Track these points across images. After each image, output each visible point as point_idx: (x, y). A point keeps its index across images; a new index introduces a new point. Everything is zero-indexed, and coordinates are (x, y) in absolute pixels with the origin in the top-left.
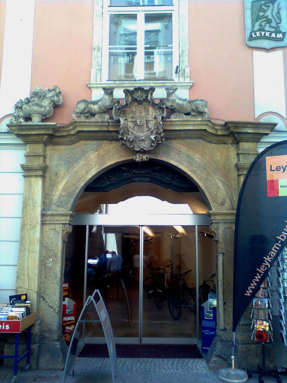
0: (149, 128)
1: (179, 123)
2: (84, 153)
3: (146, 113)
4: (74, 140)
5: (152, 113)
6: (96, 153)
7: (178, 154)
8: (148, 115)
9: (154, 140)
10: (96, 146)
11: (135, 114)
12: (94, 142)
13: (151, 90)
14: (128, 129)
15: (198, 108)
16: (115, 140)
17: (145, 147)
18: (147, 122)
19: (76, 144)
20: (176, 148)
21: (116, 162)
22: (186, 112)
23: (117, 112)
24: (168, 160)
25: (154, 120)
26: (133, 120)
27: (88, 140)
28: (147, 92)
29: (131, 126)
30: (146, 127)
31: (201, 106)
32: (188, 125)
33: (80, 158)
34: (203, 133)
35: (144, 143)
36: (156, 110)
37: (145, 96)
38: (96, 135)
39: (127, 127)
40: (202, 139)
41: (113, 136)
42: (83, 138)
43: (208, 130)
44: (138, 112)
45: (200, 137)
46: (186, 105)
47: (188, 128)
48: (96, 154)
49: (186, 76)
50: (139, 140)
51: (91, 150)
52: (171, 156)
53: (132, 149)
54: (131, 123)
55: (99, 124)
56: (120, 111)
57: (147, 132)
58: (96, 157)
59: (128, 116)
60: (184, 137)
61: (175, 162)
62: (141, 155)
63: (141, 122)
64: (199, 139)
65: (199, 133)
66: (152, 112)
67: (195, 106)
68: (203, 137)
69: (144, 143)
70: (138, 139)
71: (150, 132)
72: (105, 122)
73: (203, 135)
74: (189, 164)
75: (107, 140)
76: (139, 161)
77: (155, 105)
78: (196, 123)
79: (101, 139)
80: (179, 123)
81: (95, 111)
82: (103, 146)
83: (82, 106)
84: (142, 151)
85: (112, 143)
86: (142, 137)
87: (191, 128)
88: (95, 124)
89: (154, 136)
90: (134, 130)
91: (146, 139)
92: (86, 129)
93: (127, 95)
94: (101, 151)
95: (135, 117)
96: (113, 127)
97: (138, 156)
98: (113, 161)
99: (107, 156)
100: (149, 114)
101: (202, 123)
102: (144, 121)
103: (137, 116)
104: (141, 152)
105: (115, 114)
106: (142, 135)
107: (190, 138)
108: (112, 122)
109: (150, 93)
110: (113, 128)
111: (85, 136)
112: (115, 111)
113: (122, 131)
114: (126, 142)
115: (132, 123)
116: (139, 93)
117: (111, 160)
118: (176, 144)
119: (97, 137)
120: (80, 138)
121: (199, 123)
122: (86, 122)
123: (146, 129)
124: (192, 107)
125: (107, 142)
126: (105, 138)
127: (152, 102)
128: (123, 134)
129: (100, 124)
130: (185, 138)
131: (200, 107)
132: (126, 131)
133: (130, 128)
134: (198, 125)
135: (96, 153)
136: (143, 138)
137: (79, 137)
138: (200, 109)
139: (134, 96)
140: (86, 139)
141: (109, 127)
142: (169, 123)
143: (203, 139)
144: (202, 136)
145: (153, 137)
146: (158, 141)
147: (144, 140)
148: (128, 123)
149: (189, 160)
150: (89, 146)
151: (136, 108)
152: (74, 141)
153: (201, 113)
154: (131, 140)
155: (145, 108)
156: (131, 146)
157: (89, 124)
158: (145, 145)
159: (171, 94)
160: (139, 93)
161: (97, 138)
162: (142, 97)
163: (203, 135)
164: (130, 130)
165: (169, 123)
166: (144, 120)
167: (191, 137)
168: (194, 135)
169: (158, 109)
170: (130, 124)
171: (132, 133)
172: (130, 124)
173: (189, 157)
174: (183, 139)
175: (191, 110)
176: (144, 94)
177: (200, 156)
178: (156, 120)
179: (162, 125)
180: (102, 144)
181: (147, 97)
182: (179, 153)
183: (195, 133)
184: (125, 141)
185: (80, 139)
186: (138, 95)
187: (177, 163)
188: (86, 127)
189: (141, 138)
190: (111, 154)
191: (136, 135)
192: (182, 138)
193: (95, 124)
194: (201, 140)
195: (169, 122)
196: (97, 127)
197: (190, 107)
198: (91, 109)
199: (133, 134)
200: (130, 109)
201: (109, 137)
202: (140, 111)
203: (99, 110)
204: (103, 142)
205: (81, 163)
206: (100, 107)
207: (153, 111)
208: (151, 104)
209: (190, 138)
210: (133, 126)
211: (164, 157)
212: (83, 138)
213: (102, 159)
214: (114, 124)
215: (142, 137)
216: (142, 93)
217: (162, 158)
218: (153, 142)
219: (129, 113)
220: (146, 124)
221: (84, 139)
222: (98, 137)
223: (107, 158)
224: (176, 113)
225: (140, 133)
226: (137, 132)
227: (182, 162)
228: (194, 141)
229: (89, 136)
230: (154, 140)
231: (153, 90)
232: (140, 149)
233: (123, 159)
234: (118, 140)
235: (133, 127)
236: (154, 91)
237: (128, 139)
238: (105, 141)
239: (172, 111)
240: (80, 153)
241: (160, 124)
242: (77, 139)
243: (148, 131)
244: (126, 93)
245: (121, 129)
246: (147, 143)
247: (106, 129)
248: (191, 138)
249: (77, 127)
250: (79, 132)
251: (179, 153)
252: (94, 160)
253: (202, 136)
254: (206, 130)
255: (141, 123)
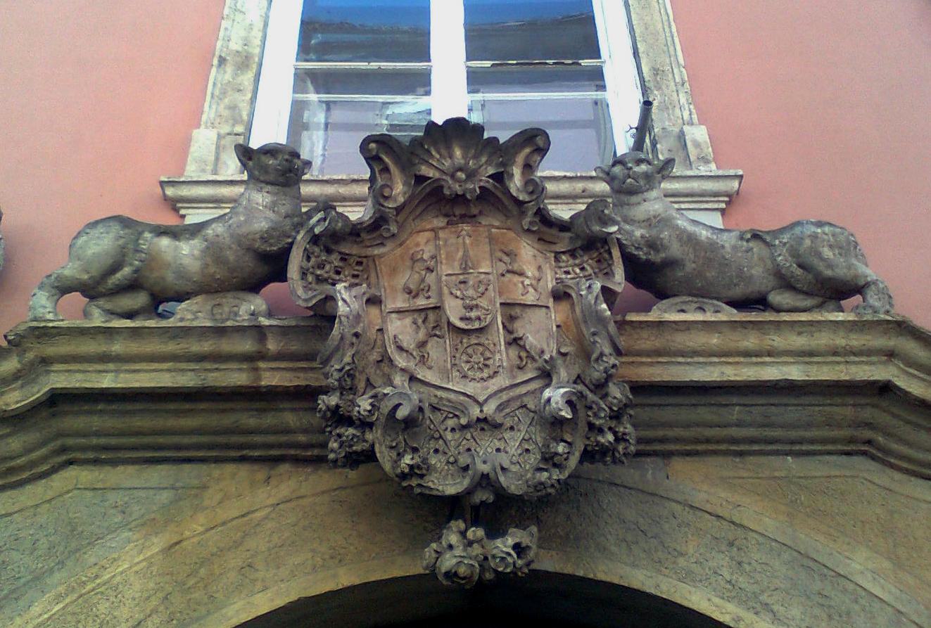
0: (523, 348)
1: (714, 340)
2: (75, 541)
3: (502, 267)
4: (19, 461)
5: (539, 268)
6: (157, 544)
7: (731, 544)
8: (516, 279)
9: (566, 414)
10: (165, 496)
11: (430, 270)
12: (157, 475)
13: (522, 147)
14: (385, 359)
15: (815, 262)
16: (297, 461)
17: (503, 469)
18: (512, 311)
19: (29, 487)
20: (708, 507)
21: (293, 597)
22: (738, 292)
23: (321, 266)
24: (664, 587)
25: (551, 303)
26: (421, 302)
27: (114, 463)
28: (501, 152)
29: (408, 341)
30: (509, 344)
31: (831, 246)
32: (770, 354)
33: (38, 579)
34: (867, 414)
35: (498, 444)
36: (557, 260)
37: (491, 171)
38: (172, 422)
39: (379, 349)
40: (864, 453)
41: (288, 431)
42: (83, 449)
43: (901, 382)
44: (450, 257)
45: (851, 441)
46: (734, 248)
47: (771, 373)
48: (156, 550)
49: (692, 158)
50: (464, 421)
51: (125, 525)
52: (682, 562)
53: (414, 482)
54: (408, 321)
55: (197, 347)
56: (335, 259)
57: (514, 377)
58: (154, 569)
59: (385, 282)
60: (753, 441)
61: (717, 600)
62: (476, 533)
63: (471, 308)
64: (848, 454)
65: (845, 411)
66: (536, 269)
67: (794, 253)
68: (869, 442)
69: (498, 444)
70: (451, 423)
71: (530, 375)
72: (239, 330)
73: (869, 425)
74: (817, 611)
75: (243, 459)
76: (462, 571)
77: (554, 231)
78: (823, 340)
79: (201, 454)
80: (714, 340)
81: (181, 273)
82: (211, 497)
83: (101, 245)
84: (483, 496)
85: (273, 482)
86: (481, 405)
87: (795, 372)
88: (171, 347)
89: (562, 391)
90: (423, 360)
91: (508, 422)
92: (107, 381)
93: (386, 169)
94: (195, 526)
95: (434, 287)
96: (283, 365)
97: (454, 538)
98: (269, 594)
99: (235, 560)
100: (521, 274)
101: (856, 341)
102: (490, 305)
103: (444, 278)
104: (476, 509)
105: (304, 274)
106: (483, 390)
107: (787, 447)
108: (284, 331)
109: (520, 159)
110: (288, 375)
111: (97, 434)
112: (308, 259)
113: (347, 359)
114: (369, 436)
115: (415, 323)
116: (458, 153)
117: (259, 586)
118: (698, 483)
119: (176, 439)
120: (64, 450)
121: (840, 341)
122: (109, 332)
123: (504, 356)
124: (774, 260)
125: (243, 471)
126: (228, 447)
127: (531, 209)
128: (348, 386)
129: (206, 346)
130: (756, 447)
131: (827, 253)
132: (371, 371)
133: (400, 348)
134: (835, 354)
135: (157, 544)
136: (490, 409)
137: (59, 443)
138: (830, 266)
139: (425, 171)
140: (106, 455)
141: (262, 365)
142: (647, 341)
143: (873, 458)
144: (868, 434)
145: (556, 395)
146: (591, 426)
147: (497, 426)
148: (384, 322)
149: (817, 586)
150: (112, 497)
151: (437, 238)
152: (21, 469)
153: (838, 291)
154: (402, 413)
155: (492, 240)
156: (407, 459)
157: (134, 347)
158: (511, 459)
159: (642, 183)
160: (458, 153)
161: (178, 448)
162: (471, 175)
163: (869, 425)
164: (401, 361)
165: (647, 341)
166: (492, 302)
167: (792, 443)
168: (809, 425)
169: (572, 253)
170: (401, 329)
171: (413, 379)
172: (401, 329)
173: (806, 561)
174: (741, 454)
175: (769, 282)
176: (484, 159)
177: (887, 564)
178: (564, 306)
179: (612, 328)
180: (204, 487)
181: (499, 178)
182: (734, 536)
183: (817, 410)
184: (365, 425)
185: (64, 458)
186: (447, 163)
187: (731, 607)
188: (111, 366)
189: (475, 412)
190: (258, 543)
191: (439, 393)
192: (737, 449)
193: (171, 347)
194: (857, 460)
195: (645, 334)
196: (183, 366)
197: (761, 259)
198: (152, 260)
199: (416, 386)
200: (399, 251)
201: (258, 439)
202: (460, 254)
203: (207, 266)
204: (216, 470)
205: (36, 609)
206: (214, 251)
207: (540, 260)
208: (526, 223)
209: (787, 447)
210: (421, 335)
211: (634, 566)
212: (83, 449)
213: (191, 582)
214: (295, 346)
215: (481, 405)
216: (476, 157)
217: (628, 570)
218: (557, 423)
219: (394, 271)
220: (504, 327)
221: (91, 455)
222: (186, 440)
223: (232, 576)
224: (677, 300)
225: (465, 377)
226: (446, 375)
227: (764, 598)
228: (817, 468)
229: (122, 434)
230: (566, 414)
231: (540, 141)
232: (466, 483)
233: (345, 578)
234: (310, 457)
235: (422, 345)
236: (542, 151)
237: (386, 407)
238: (229, 468)
239: (651, 275)
240: (43, 544)
241: (600, 320)
242: (44, 451)
243: (520, 368)
244: (372, 159)
245: (337, 348)
246: (513, 447)
247: (237, 377)
248: (797, 447)
249: (48, 372)
250: (58, 400)
251: (734, 536)
252: (136, 588)
253: (868, 434)
254: (885, 389)
255: (473, 314)
